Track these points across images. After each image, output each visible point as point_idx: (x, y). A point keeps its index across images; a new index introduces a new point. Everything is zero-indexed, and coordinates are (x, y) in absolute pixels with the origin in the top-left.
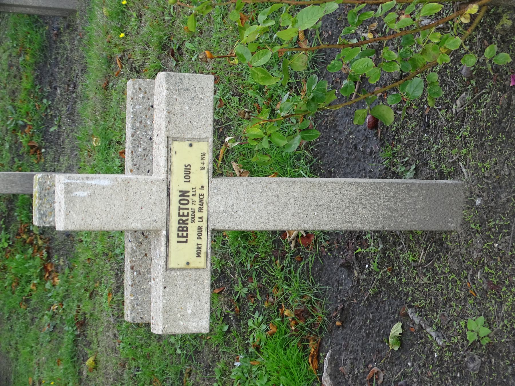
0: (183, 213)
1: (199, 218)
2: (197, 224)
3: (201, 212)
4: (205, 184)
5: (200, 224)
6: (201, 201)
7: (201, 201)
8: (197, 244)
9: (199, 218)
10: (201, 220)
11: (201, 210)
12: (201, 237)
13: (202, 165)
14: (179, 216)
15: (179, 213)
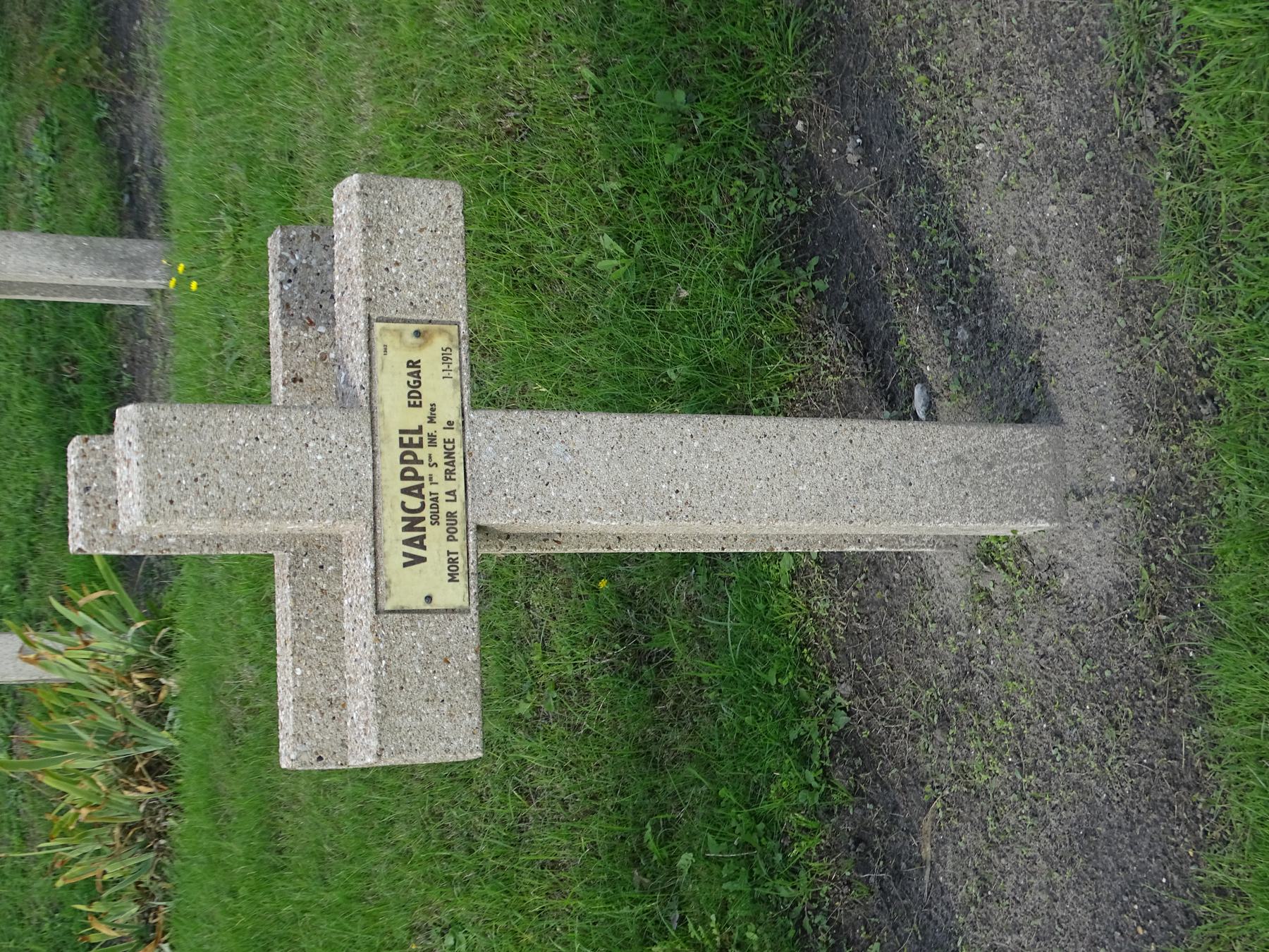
0: (411, 439)
1: (448, 493)
2: (445, 507)
3: (451, 479)
4: (454, 416)
5: (452, 507)
6: (449, 454)
7: (449, 454)
8: (449, 553)
9: (448, 493)
10: (452, 498)
11: (449, 475)
12: (456, 536)
13: (446, 374)
14: (402, 445)
15: (401, 439)
